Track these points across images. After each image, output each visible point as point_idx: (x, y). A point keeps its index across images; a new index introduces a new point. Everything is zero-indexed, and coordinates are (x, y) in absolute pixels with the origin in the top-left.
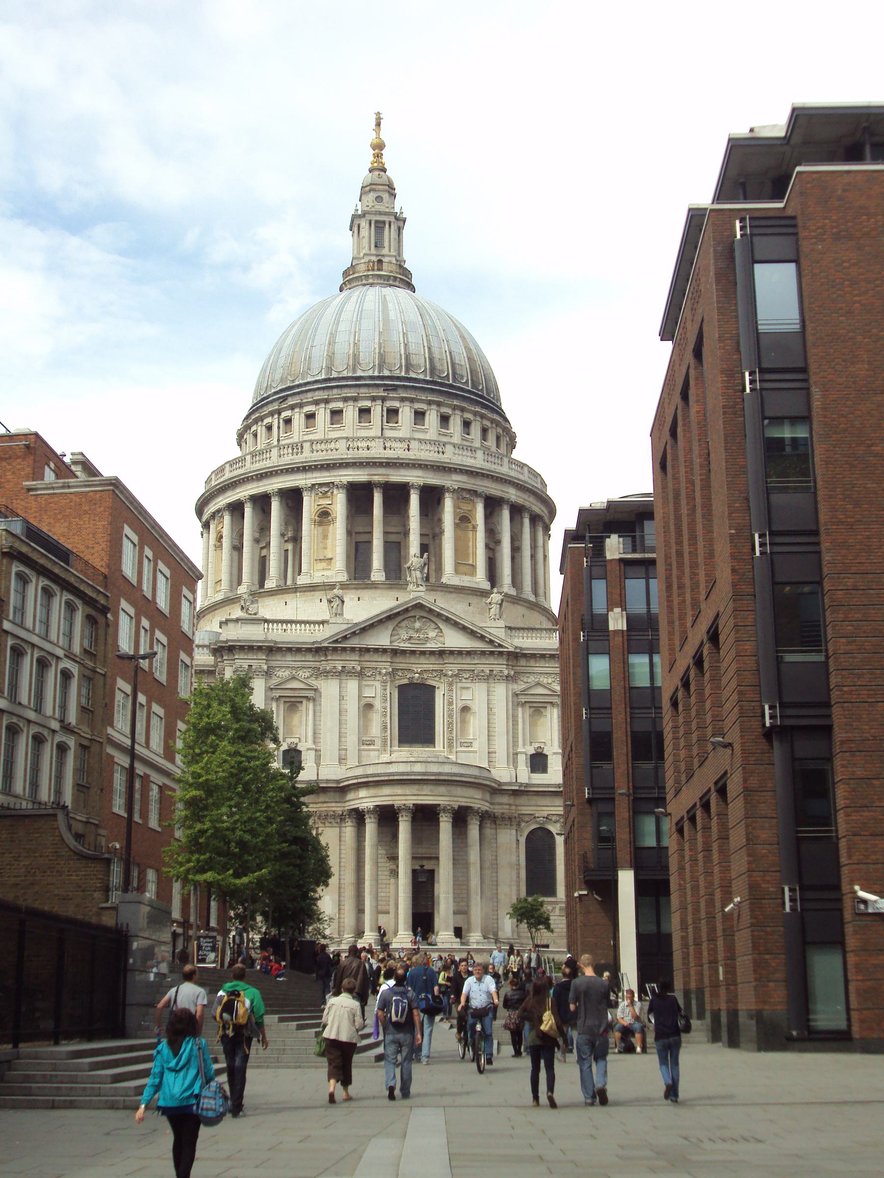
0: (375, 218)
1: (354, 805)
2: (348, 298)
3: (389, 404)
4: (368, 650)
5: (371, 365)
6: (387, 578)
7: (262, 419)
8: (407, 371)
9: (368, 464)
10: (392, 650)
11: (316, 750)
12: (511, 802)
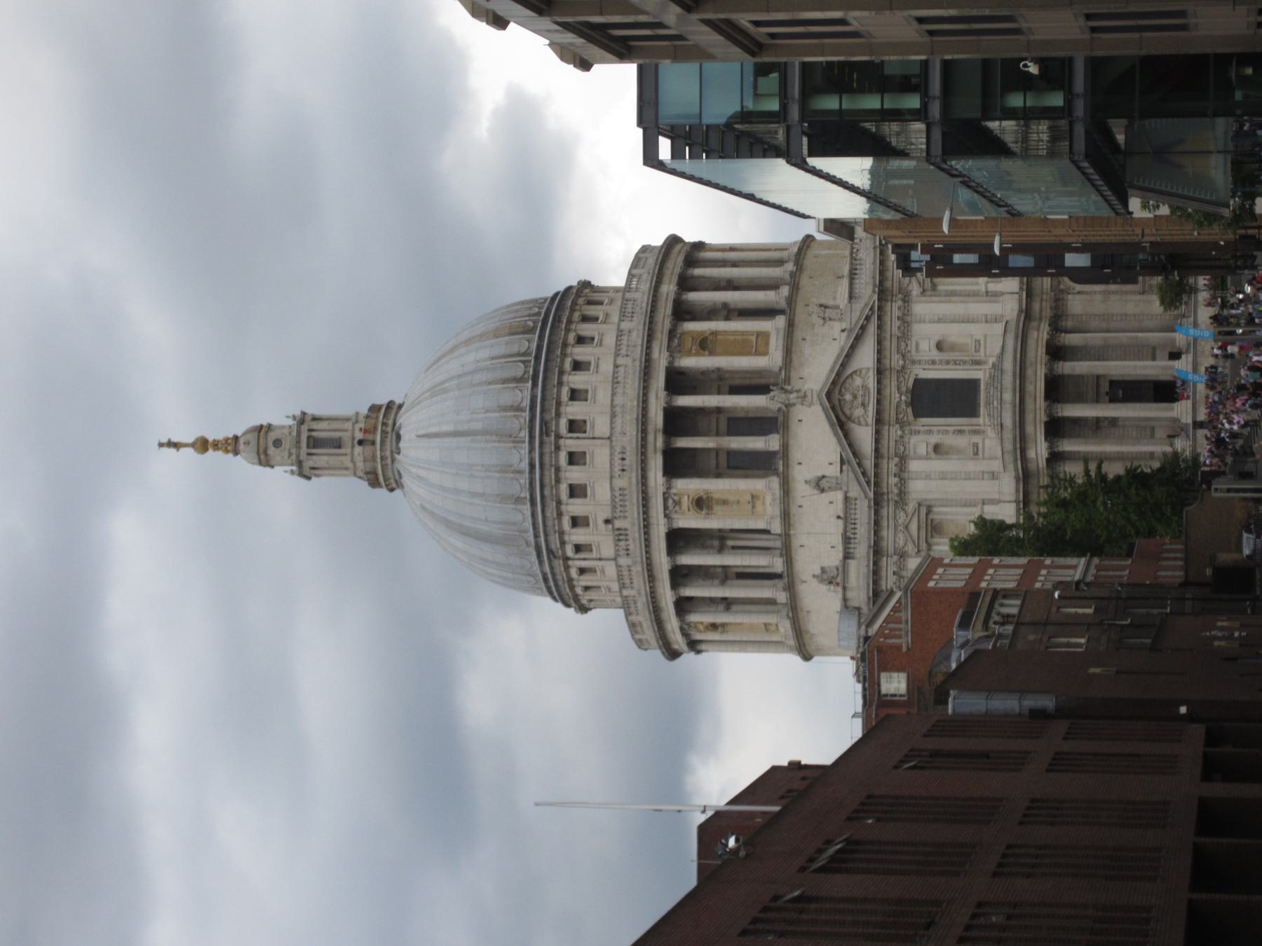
0: (304, 450)
1: (1042, 463)
2: (419, 478)
4: (877, 450)
5: (514, 451)
6: (778, 433)
7: (570, 580)
10: (876, 424)
11: (984, 504)
12: (1039, 299)
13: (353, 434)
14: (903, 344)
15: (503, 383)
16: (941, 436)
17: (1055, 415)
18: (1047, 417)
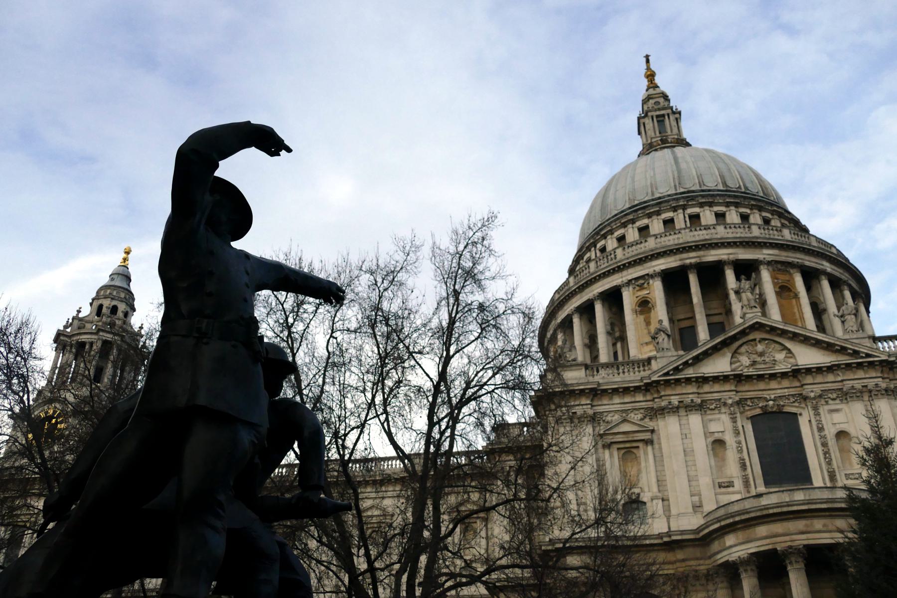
1: (722, 558)
3: (690, 211)
4: (704, 380)
8: (700, 187)
9: (678, 249)
10: (736, 376)
11: (663, 500)
13: (670, 135)
14: (834, 396)
15: (720, 175)
16: (735, 445)
17: (787, 562)
18: (783, 551)
